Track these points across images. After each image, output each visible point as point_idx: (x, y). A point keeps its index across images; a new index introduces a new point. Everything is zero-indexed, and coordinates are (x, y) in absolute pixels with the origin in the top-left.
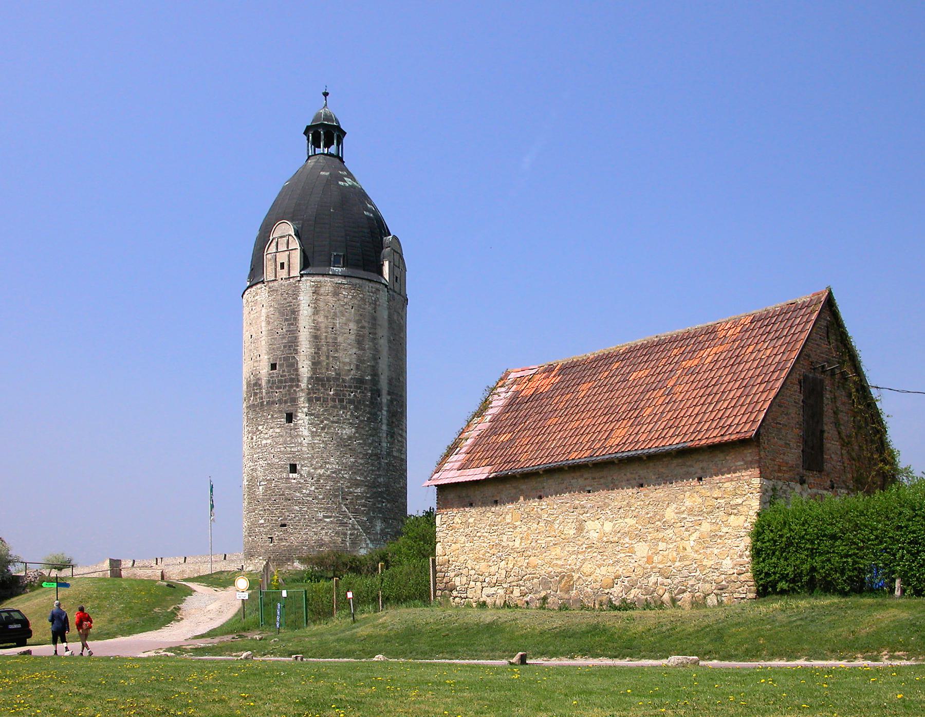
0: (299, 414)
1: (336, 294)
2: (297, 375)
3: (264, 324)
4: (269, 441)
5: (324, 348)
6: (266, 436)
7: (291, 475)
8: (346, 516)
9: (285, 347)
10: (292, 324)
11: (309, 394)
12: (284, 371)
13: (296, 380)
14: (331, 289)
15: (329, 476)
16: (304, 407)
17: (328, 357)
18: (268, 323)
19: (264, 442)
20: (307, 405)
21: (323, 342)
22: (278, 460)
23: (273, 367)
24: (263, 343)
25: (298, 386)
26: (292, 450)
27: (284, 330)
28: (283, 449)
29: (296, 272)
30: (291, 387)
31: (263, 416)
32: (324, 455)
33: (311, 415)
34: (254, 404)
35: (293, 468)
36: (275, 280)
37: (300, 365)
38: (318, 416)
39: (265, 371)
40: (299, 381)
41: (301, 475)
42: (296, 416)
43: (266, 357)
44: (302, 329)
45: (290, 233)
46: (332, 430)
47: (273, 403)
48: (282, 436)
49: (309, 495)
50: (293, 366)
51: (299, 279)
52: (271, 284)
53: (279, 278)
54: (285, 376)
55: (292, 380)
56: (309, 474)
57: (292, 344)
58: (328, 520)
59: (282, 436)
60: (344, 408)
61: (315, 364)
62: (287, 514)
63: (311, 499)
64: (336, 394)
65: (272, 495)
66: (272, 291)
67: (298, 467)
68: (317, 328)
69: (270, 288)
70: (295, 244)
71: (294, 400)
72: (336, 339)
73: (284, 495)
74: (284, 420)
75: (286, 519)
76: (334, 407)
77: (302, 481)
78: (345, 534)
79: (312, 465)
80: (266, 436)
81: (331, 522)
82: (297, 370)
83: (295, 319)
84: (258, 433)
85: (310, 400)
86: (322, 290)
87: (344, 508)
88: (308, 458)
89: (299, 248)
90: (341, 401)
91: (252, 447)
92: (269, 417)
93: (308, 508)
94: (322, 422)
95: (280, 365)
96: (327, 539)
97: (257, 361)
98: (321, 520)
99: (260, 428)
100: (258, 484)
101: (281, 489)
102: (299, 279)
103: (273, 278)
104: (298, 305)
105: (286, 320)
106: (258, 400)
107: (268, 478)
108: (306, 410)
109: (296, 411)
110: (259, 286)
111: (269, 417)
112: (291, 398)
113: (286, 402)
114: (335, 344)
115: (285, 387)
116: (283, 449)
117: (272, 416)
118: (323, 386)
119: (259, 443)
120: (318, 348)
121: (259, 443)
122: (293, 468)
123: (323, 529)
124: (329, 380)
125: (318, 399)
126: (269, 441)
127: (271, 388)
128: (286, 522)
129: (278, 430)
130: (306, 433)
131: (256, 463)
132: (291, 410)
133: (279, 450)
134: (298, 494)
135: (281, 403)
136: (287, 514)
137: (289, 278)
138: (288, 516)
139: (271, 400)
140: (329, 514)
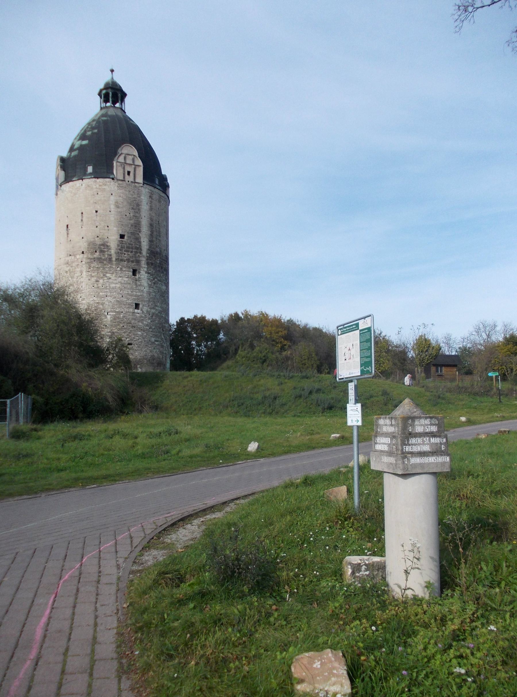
0: (142, 272)
1: (160, 202)
2: (140, 246)
3: (112, 207)
4: (118, 286)
5: (155, 233)
6: (115, 282)
7: (136, 310)
8: (163, 342)
9: (132, 225)
10: (137, 213)
11: (147, 259)
12: (131, 241)
13: (139, 249)
14: (158, 197)
15: (157, 314)
16: (145, 268)
17: (156, 238)
18: (118, 207)
19: (113, 285)
20: (146, 266)
21: (154, 229)
22: (126, 300)
23: (122, 236)
24: (112, 219)
25: (141, 253)
26: (137, 294)
27: (132, 215)
28: (130, 292)
29: (140, 179)
30: (136, 252)
31: (111, 267)
32: (155, 301)
33: (149, 273)
34: (101, 258)
35: (137, 306)
36: (124, 181)
37: (142, 240)
38: (152, 275)
39: (114, 238)
40: (141, 250)
41: (143, 312)
42: (139, 272)
43: (115, 229)
44: (143, 218)
45: (135, 154)
46: (158, 285)
47: (122, 260)
48: (129, 284)
49: (147, 325)
50: (138, 240)
51: (142, 185)
52: (120, 182)
53: (127, 180)
54: (132, 244)
55: (137, 248)
56: (147, 311)
57: (137, 226)
58: (156, 343)
59: (129, 284)
60: (163, 272)
61: (151, 241)
62: (133, 336)
63: (148, 328)
64: (160, 263)
65: (121, 323)
66: (119, 187)
67: (141, 306)
68: (151, 219)
69: (119, 184)
70: (139, 162)
71: (138, 262)
72: (159, 229)
73: (130, 323)
74: (131, 274)
75: (132, 340)
76: (159, 271)
77: (143, 316)
78: (163, 353)
79: (149, 306)
80: (115, 282)
81: (158, 345)
82: (140, 242)
83: (139, 210)
84: (106, 278)
85: (148, 264)
86: (154, 197)
87: (163, 337)
88: (147, 301)
89: (142, 166)
90: (162, 268)
91: (98, 287)
92: (119, 269)
93: (147, 334)
94: (154, 279)
95: (128, 237)
96: (156, 355)
97: (105, 230)
98: (154, 343)
99: (108, 275)
100: (106, 314)
101: (129, 319)
102: (142, 185)
103: (122, 178)
104: (141, 202)
105: (133, 208)
106: (106, 256)
107: (117, 310)
108: (146, 269)
109: (140, 269)
110: (108, 180)
111: (119, 269)
112: (136, 260)
113: (132, 262)
114: (159, 232)
115: (132, 252)
116: (130, 292)
117: (121, 269)
118: (155, 256)
119: (108, 285)
120: (152, 232)
121: (108, 285)
122: (137, 306)
123: (154, 348)
124: (157, 253)
125: (152, 264)
126: (118, 286)
127: (120, 250)
128: (132, 342)
129: (126, 279)
130: (146, 284)
131: (103, 299)
132: (136, 267)
133: (127, 292)
134: (140, 324)
135: (128, 262)
136: (133, 336)
137: (135, 182)
138: (134, 338)
139: (120, 258)
140: (157, 339)
